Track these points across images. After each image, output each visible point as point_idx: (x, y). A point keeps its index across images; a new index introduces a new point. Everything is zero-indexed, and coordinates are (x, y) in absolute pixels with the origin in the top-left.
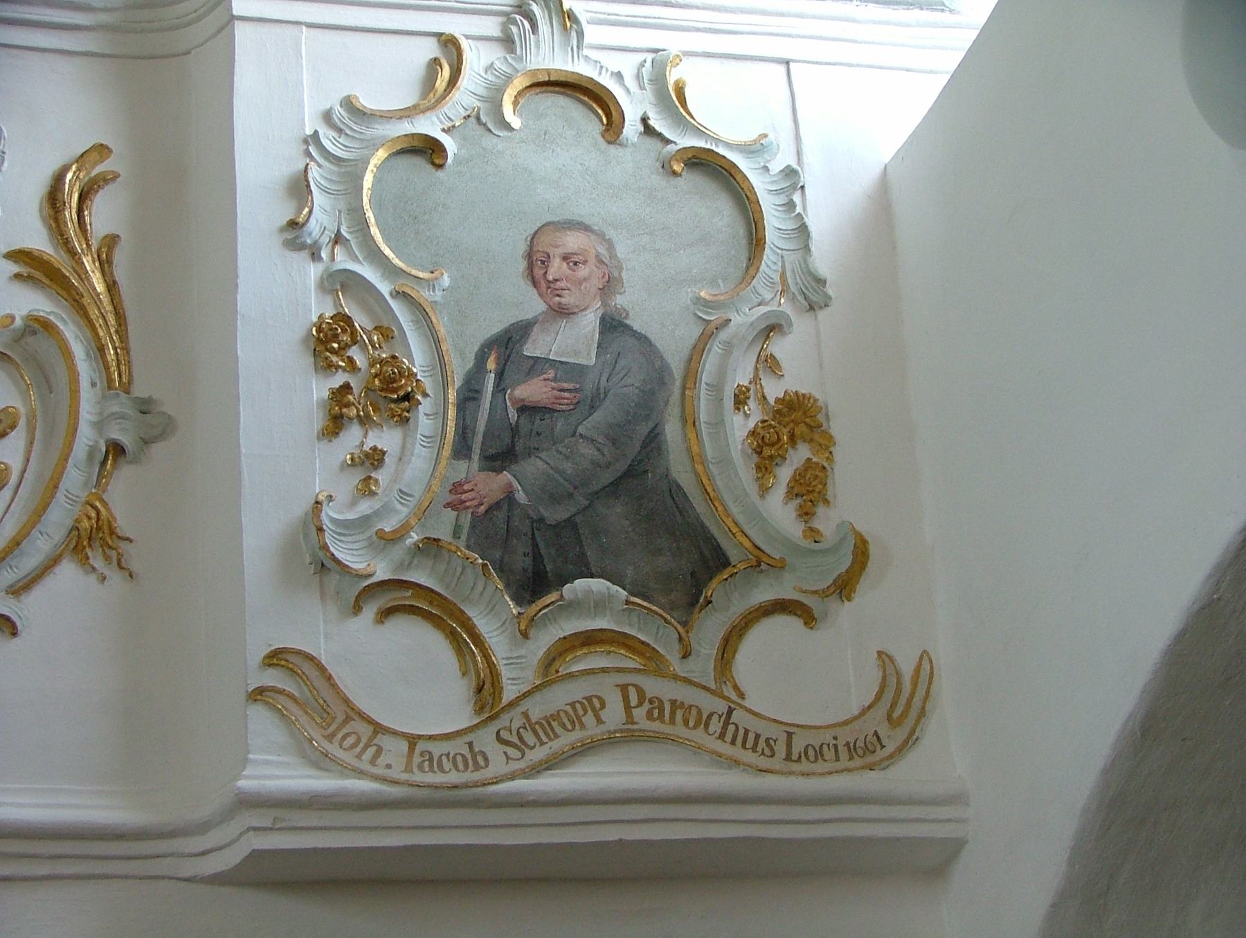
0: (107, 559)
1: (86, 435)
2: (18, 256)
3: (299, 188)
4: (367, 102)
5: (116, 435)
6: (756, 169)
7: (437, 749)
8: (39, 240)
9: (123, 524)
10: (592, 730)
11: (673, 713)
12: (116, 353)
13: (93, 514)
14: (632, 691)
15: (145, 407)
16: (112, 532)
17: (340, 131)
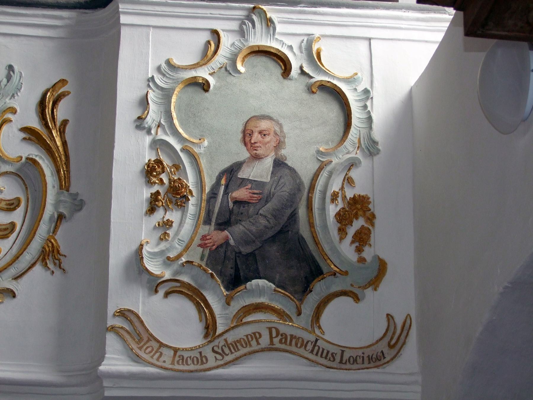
0: (55, 264)
1: (49, 210)
2: (25, 130)
3: (144, 102)
4: (177, 62)
5: (61, 210)
6: (351, 90)
7: (186, 355)
8: (35, 123)
9: (62, 250)
10: (254, 346)
11: (291, 341)
12: (64, 173)
13: (50, 245)
14: (274, 331)
15: (74, 196)
16: (58, 252)
17: (164, 75)
